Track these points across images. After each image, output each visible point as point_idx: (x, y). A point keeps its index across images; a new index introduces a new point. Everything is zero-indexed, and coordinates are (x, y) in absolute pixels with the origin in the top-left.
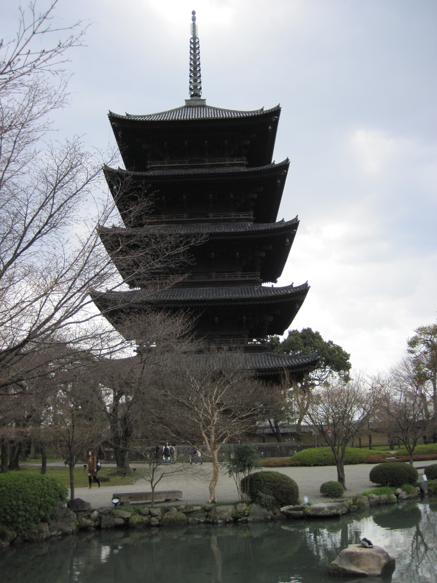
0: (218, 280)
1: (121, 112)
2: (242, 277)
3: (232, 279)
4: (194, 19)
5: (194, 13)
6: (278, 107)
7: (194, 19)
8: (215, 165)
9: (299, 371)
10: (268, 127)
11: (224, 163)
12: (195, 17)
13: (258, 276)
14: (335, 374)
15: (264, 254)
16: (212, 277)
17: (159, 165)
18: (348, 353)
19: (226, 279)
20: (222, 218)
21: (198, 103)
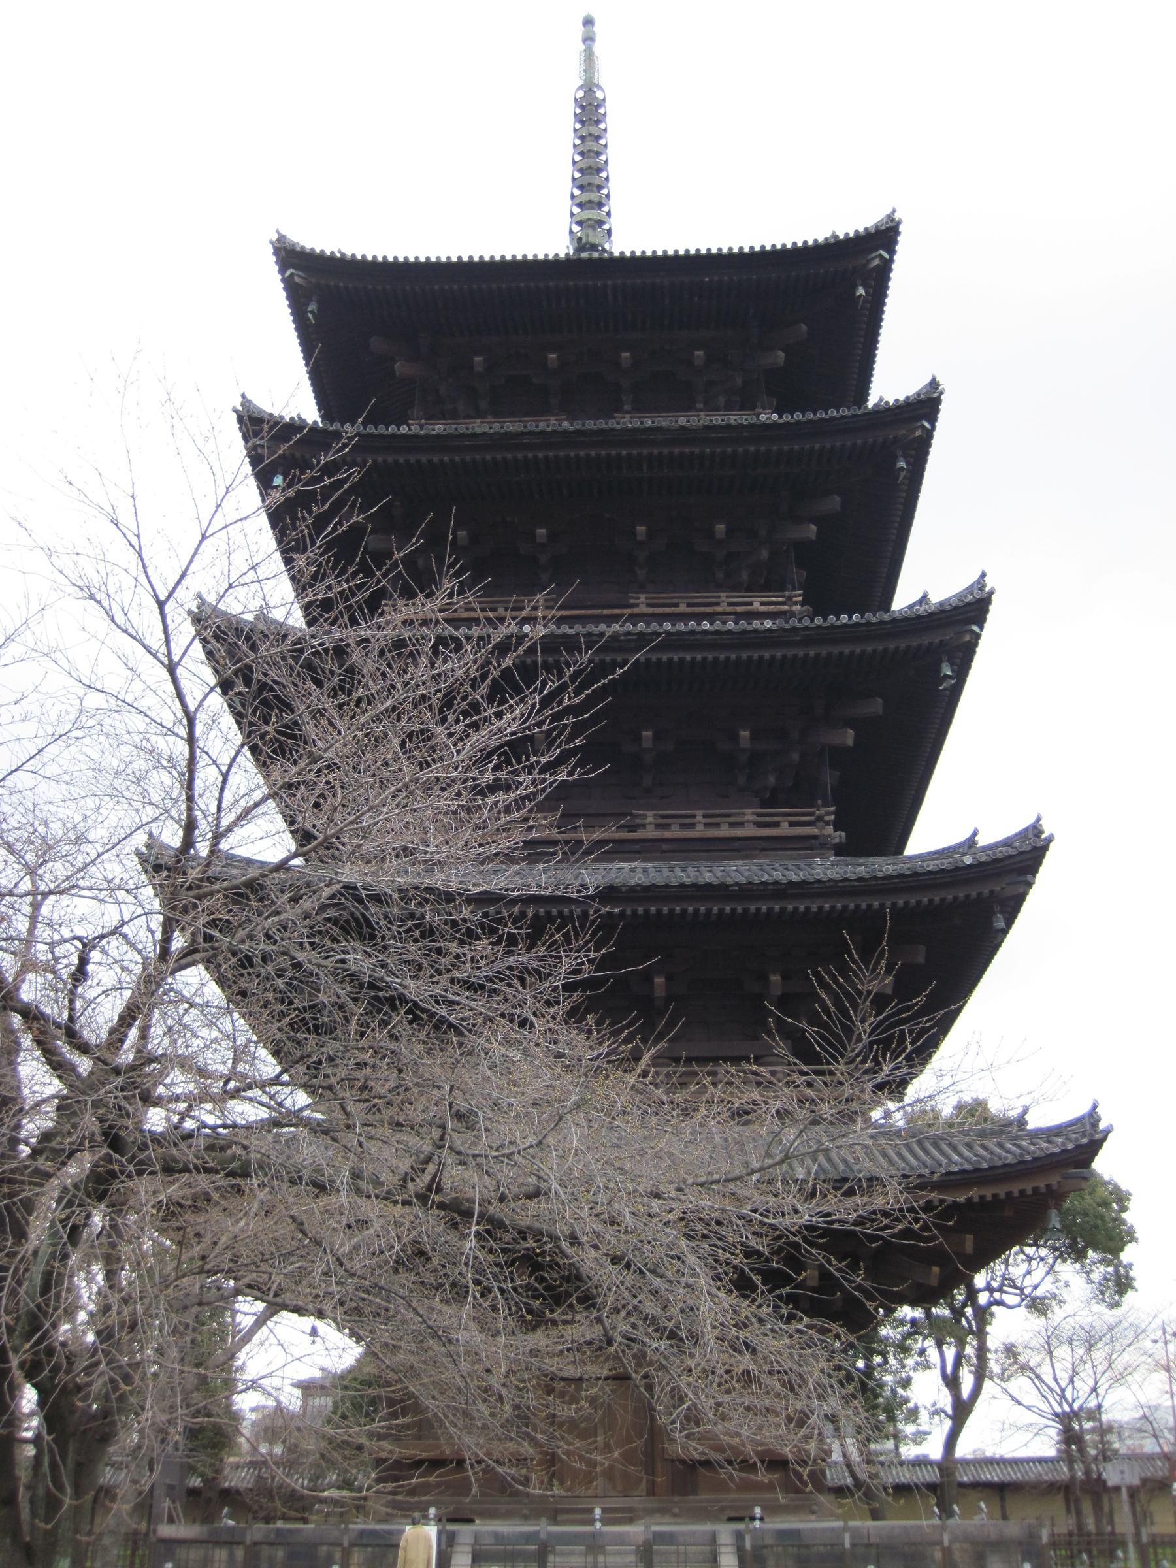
0: (667, 834)
2: (759, 825)
3: (724, 831)
4: (588, 39)
5: (588, 22)
6: (890, 217)
9: (1022, 1192)
10: (855, 287)
12: (594, 33)
13: (827, 823)
14: (1068, 1270)
15: (849, 737)
16: (644, 826)
18: (1124, 1187)
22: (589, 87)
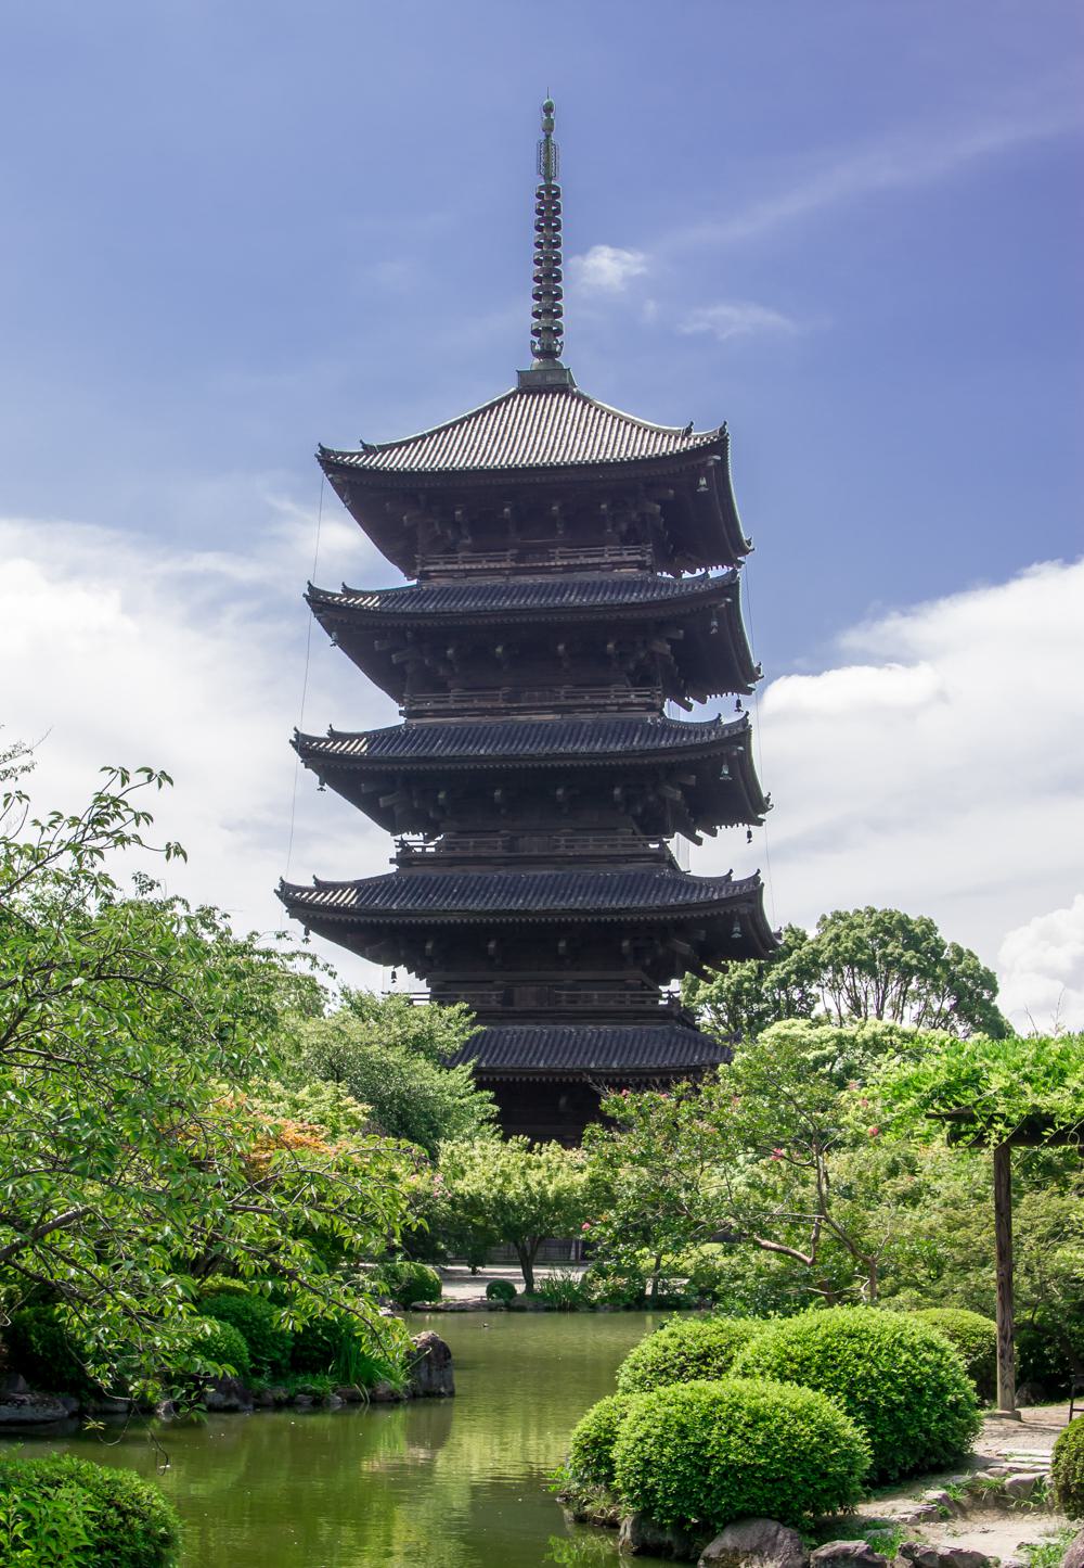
1: (347, 445)
3: (605, 850)
4: (548, 128)
5: (548, 109)
7: (548, 128)
8: (576, 565)
11: (597, 560)
17: (443, 568)
19: (591, 850)
20: (587, 700)
21: (550, 379)
22: (548, 188)
